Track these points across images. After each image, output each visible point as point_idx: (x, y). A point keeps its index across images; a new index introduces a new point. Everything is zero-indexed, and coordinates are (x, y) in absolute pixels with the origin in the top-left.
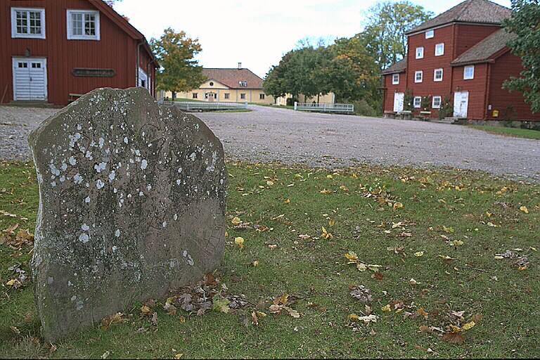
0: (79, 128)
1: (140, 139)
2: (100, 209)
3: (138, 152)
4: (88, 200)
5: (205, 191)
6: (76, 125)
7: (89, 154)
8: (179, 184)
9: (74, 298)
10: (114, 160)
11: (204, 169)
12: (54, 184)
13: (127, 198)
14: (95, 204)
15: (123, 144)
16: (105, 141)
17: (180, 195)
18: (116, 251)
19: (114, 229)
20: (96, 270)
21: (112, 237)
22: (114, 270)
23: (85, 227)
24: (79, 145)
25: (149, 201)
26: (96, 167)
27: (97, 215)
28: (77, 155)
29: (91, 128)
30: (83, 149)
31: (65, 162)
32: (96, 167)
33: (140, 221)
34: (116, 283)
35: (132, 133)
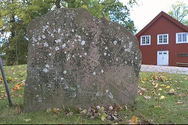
0: (48, 23)
1: (81, 31)
2: (56, 59)
3: (79, 37)
4: (50, 54)
5: (124, 61)
6: (47, 22)
7: (52, 35)
8: (105, 55)
9: (37, 96)
10: (65, 39)
11: (123, 50)
12: (34, 45)
13: (72, 57)
14: (54, 57)
15: (71, 32)
16: (61, 30)
17: (106, 61)
18: (63, 80)
19: (63, 70)
20: (50, 86)
21: (62, 74)
22: (60, 89)
23: (47, 66)
24: (47, 30)
25: (85, 60)
26: (56, 41)
27: (55, 62)
28: (46, 35)
29: (54, 24)
30: (49, 32)
31: (40, 37)
32: (56, 41)
33: (79, 69)
34: (61, 95)
35: (77, 28)
